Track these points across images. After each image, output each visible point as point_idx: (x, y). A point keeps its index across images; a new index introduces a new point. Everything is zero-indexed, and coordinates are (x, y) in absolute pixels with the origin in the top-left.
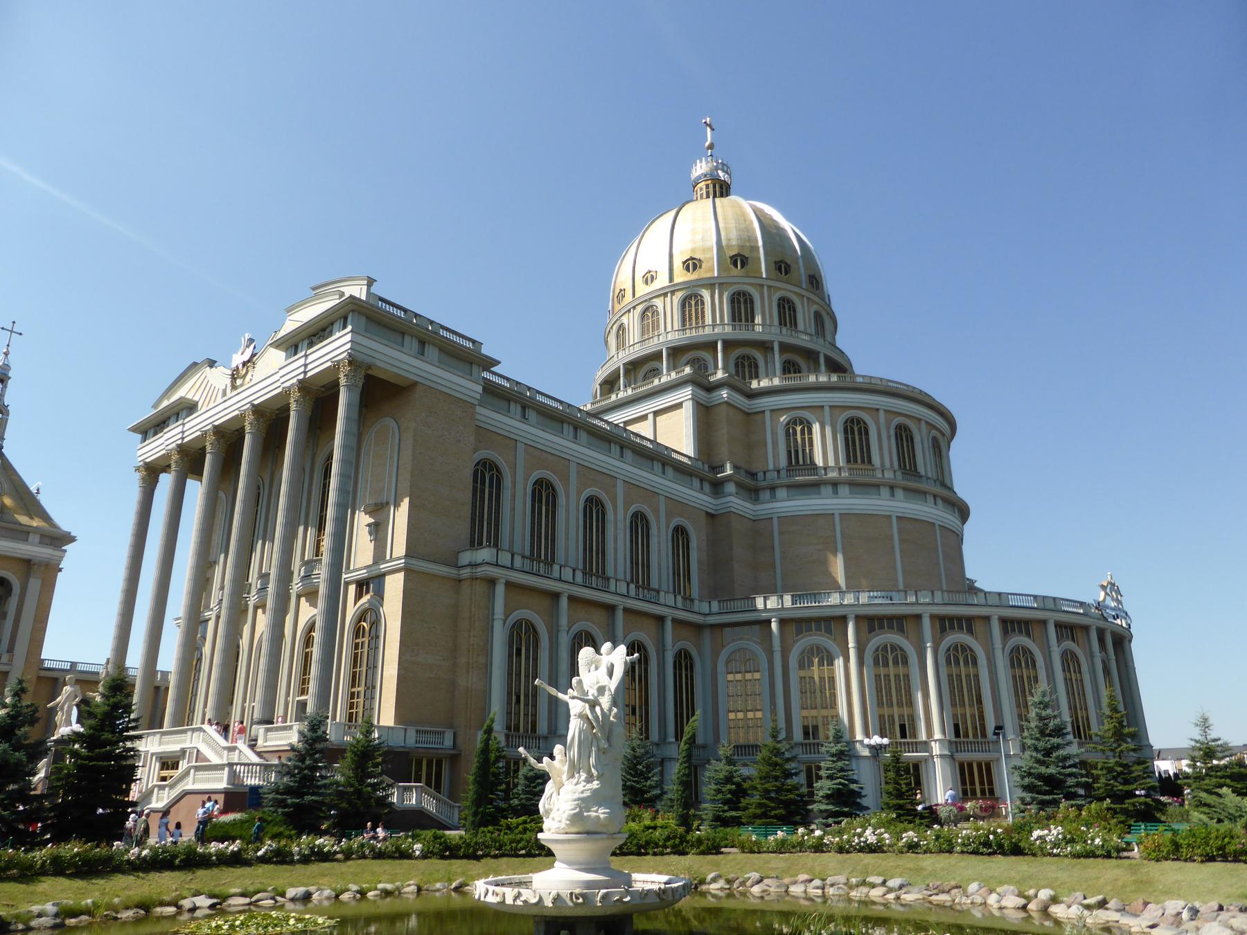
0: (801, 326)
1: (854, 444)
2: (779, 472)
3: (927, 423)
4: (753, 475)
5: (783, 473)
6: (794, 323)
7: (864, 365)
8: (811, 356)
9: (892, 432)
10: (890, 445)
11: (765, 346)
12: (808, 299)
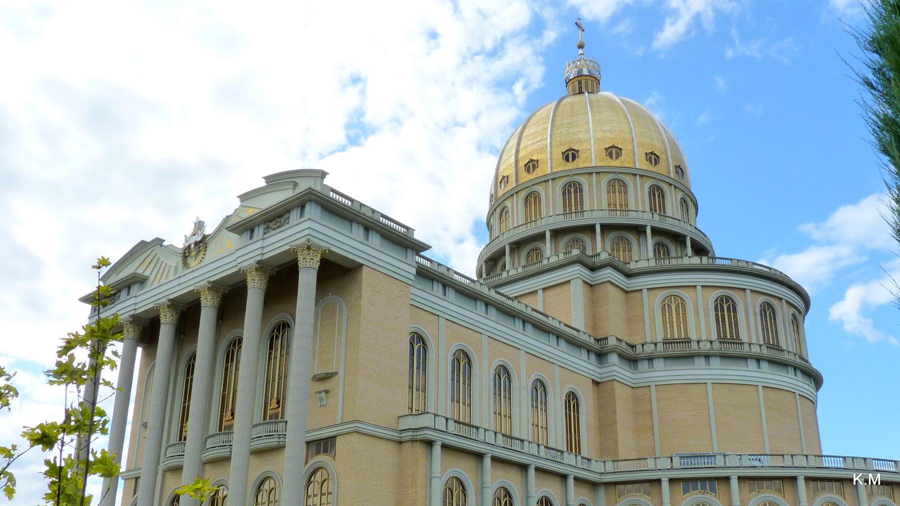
0: (669, 213)
1: (723, 321)
2: (656, 344)
3: (787, 302)
4: (633, 347)
5: (660, 347)
6: (663, 208)
7: (724, 248)
8: (678, 239)
9: (758, 310)
10: (755, 322)
11: (638, 230)
12: (675, 187)
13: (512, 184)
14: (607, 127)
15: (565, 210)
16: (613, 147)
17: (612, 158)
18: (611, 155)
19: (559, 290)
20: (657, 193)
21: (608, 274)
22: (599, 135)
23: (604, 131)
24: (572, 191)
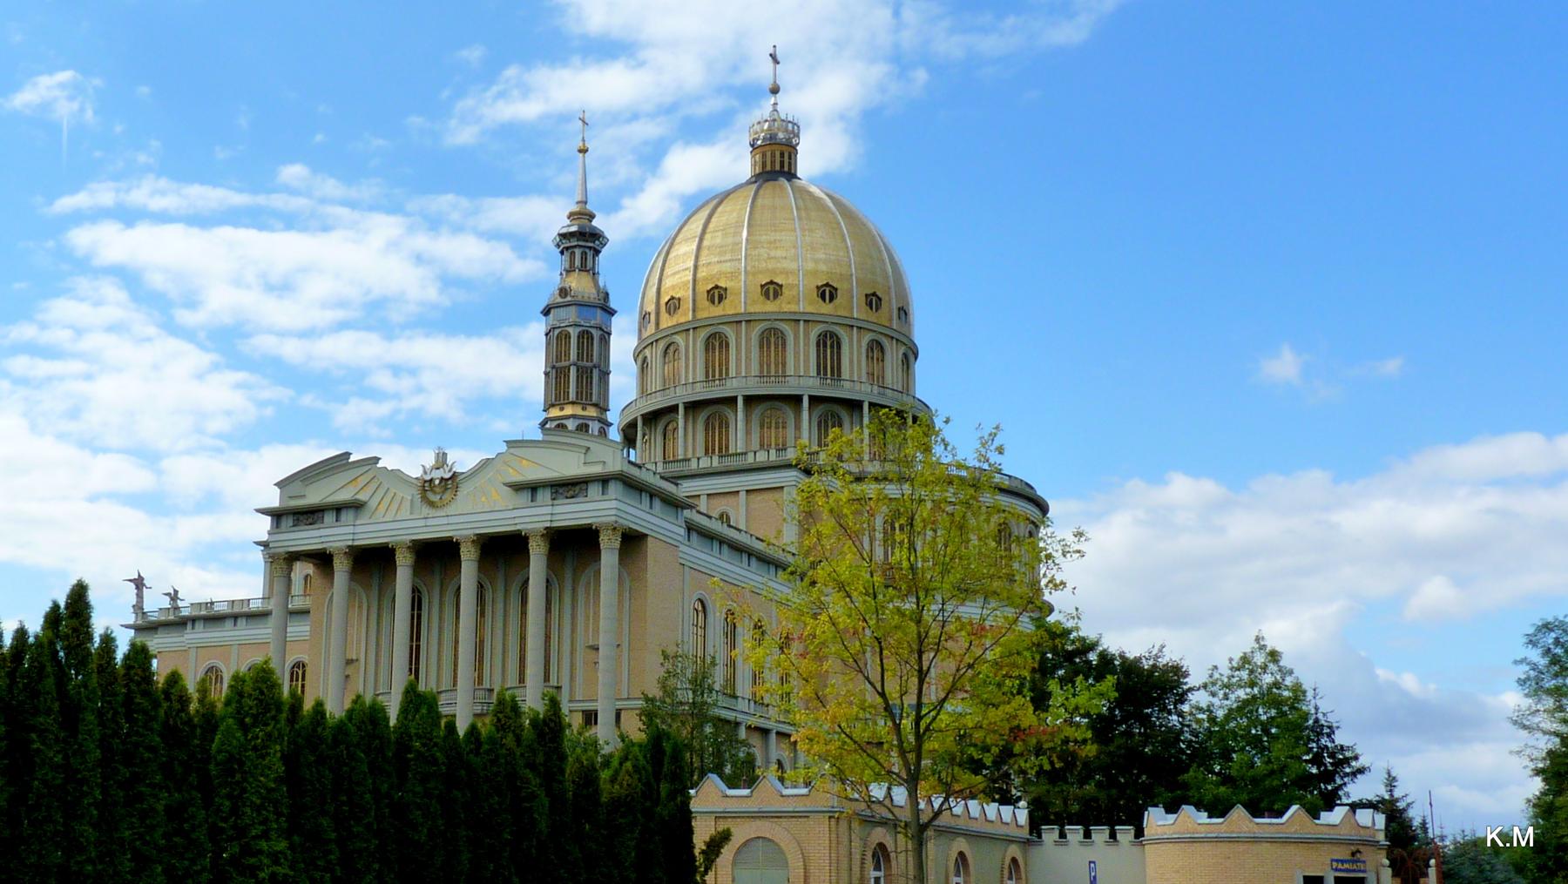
0: (889, 381)
11: (854, 406)
13: (684, 316)
14: (821, 256)
16: (827, 285)
17: (824, 299)
18: (823, 297)
19: (765, 496)
22: (810, 266)
23: (816, 261)
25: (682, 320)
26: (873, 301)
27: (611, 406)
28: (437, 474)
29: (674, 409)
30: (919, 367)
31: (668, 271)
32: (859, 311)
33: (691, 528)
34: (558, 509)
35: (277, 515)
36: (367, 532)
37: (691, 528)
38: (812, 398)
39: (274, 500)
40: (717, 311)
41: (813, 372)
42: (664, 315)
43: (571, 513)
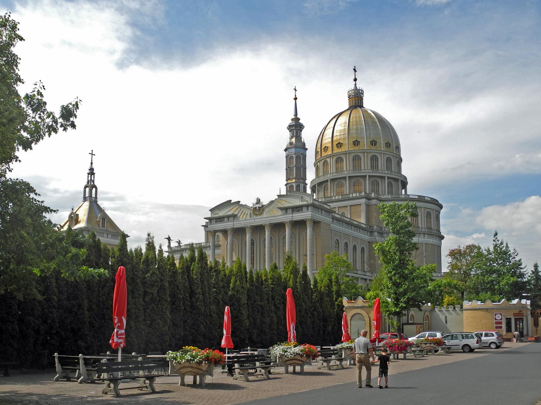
8: (396, 180)
11: (383, 178)
13: (329, 152)
15: (354, 168)
20: (389, 160)
21: (374, 202)
24: (356, 159)
25: (329, 153)
26: (388, 145)
27: (307, 178)
28: (258, 206)
29: (327, 181)
30: (403, 165)
31: (324, 138)
32: (383, 148)
33: (334, 218)
34: (294, 215)
35: (210, 219)
36: (237, 224)
37: (334, 218)
38: (369, 176)
39: (209, 215)
40: (340, 150)
41: (369, 168)
42: (323, 152)
43: (298, 216)
